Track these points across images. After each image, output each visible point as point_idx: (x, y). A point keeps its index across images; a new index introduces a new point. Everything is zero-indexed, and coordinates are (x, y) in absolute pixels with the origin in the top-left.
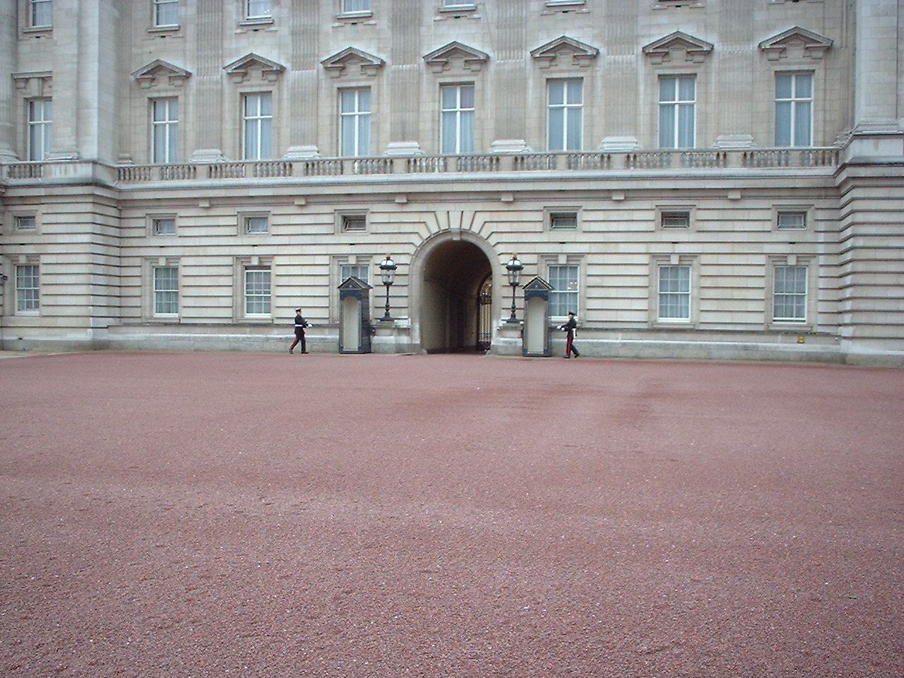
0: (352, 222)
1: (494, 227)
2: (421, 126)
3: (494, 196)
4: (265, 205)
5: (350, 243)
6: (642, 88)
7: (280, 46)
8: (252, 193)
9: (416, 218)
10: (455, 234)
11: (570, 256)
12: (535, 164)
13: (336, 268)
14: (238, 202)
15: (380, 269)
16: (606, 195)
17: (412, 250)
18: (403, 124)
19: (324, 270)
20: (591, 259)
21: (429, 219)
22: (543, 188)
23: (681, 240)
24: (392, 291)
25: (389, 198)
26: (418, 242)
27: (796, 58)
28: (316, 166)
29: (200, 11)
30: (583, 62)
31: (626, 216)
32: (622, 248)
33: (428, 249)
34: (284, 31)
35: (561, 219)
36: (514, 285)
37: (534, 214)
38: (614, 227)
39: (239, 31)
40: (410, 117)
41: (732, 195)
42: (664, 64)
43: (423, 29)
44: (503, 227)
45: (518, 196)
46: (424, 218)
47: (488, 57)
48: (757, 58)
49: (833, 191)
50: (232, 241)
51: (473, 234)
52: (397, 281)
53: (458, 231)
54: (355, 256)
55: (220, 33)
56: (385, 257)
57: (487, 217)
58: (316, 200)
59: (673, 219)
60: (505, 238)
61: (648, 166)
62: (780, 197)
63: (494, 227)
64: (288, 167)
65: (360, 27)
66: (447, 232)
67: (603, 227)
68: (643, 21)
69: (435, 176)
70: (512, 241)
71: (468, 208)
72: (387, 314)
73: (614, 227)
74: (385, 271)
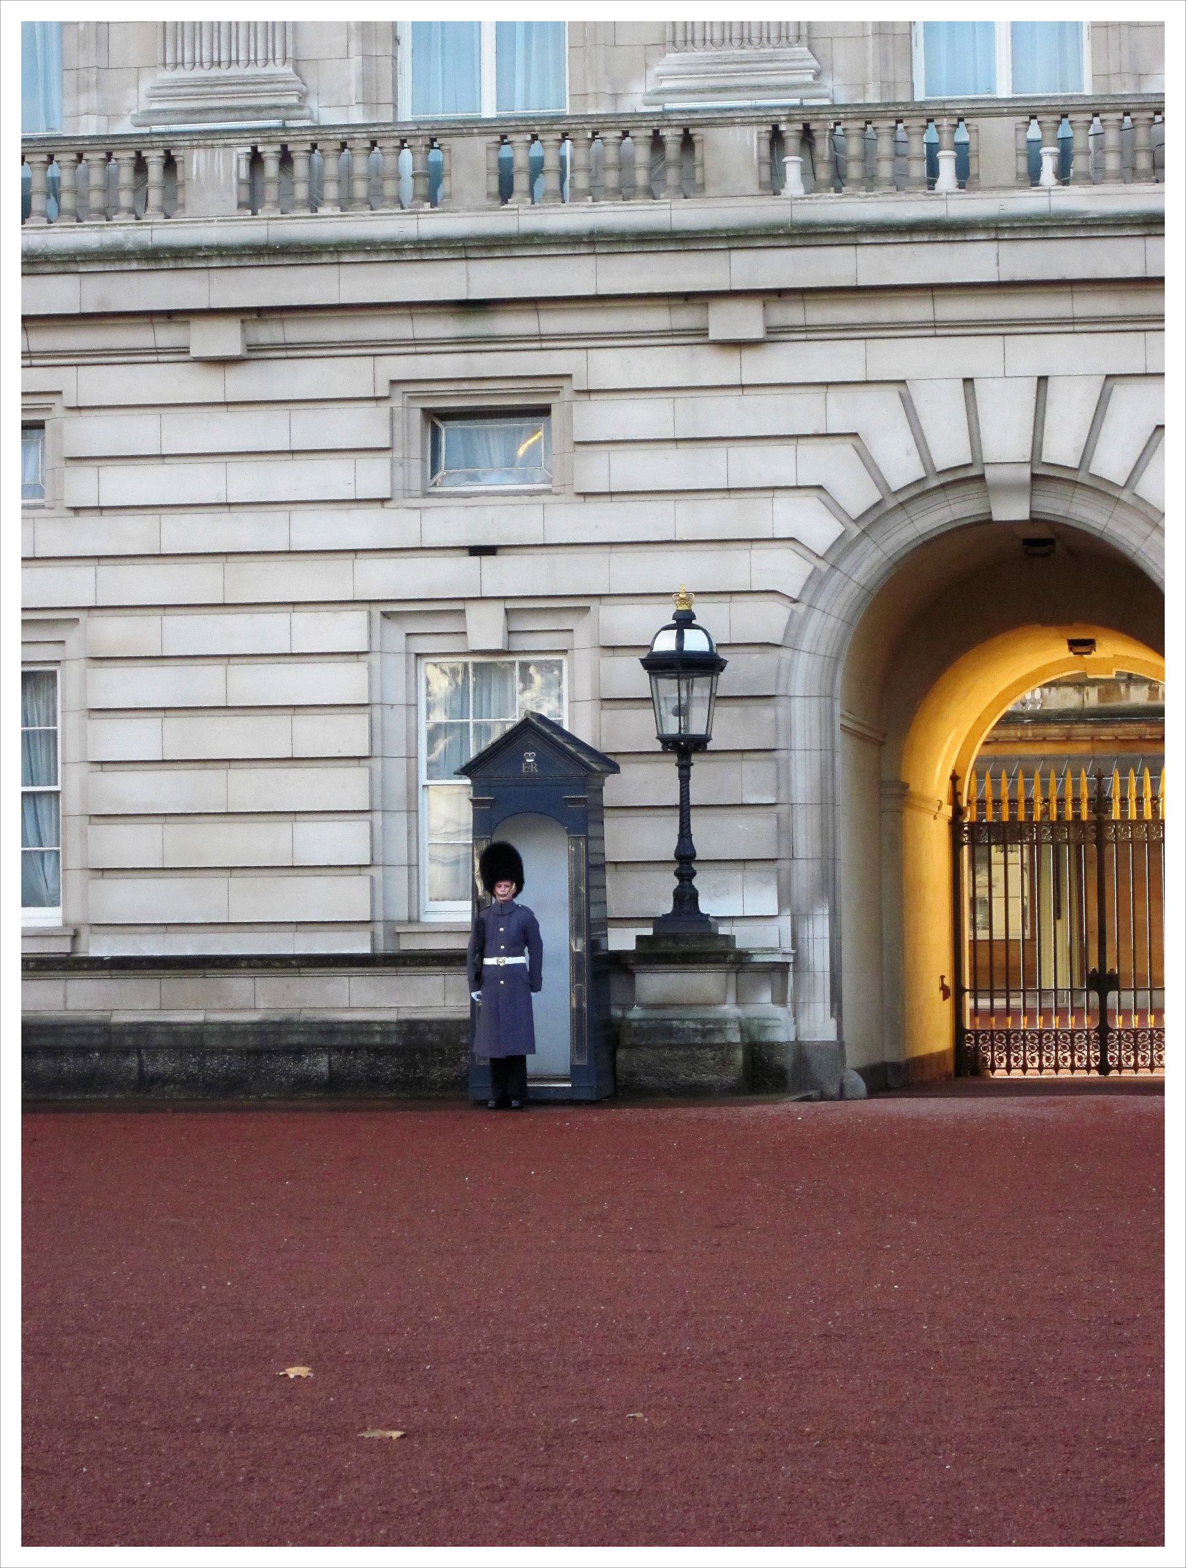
9: (804, 413)
10: (1009, 488)
13: (396, 665)
15: (645, 674)
17: (786, 571)
19: (346, 683)
21: (877, 417)
24: (707, 779)
26: (822, 530)
28: (300, 167)
33: (869, 564)
46: (839, 412)
51: (1101, 490)
52: (727, 729)
53: (1026, 473)
54: (498, 609)
56: (666, 613)
64: (155, 171)
66: (969, 478)
74: (668, 686)
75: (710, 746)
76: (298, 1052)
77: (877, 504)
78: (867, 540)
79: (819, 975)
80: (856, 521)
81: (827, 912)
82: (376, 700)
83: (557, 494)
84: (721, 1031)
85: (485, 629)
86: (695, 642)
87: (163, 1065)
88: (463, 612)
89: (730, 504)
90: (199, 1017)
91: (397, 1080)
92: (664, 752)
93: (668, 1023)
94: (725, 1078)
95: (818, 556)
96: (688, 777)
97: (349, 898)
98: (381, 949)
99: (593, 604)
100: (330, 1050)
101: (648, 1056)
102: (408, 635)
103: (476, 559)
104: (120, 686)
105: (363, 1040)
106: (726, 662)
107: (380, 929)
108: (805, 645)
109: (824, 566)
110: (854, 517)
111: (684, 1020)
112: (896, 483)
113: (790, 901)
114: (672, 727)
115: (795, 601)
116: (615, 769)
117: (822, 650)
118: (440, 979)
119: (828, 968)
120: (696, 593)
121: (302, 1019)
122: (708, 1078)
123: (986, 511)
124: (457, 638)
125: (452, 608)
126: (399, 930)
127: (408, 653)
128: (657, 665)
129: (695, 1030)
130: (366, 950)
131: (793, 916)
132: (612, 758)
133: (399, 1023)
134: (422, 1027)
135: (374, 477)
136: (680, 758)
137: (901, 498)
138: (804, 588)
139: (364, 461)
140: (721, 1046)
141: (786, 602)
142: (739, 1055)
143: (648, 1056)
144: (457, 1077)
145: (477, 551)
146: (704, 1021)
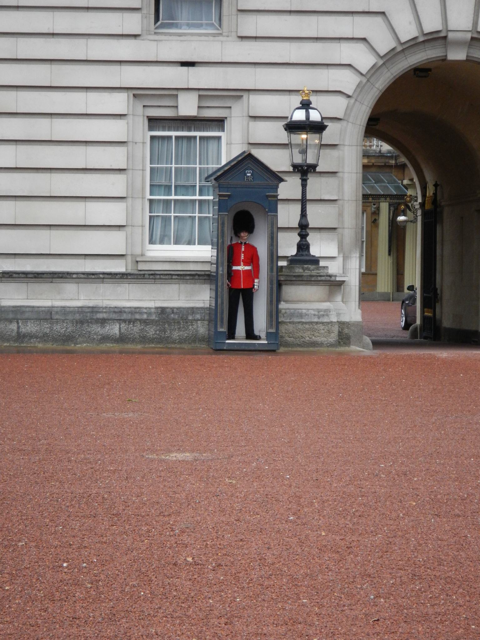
10: (459, 44)
17: (347, 81)
24: (317, 187)
26: (365, 60)
53: (469, 36)
56: (296, 100)
72: (303, 247)
75: (318, 169)
76: (103, 322)
77: (393, 49)
78: (384, 66)
79: (353, 288)
80: (382, 57)
81: (358, 255)
82: (130, 139)
83: (228, 36)
84: (327, 315)
85: (188, 107)
86: (315, 116)
87: (30, 328)
88: (176, 96)
89: (318, 45)
90: (48, 303)
91: (155, 338)
92: (294, 172)
93: (300, 311)
94: (330, 340)
95: (361, 74)
96: (306, 185)
97: (114, 242)
98: (129, 271)
99: (245, 95)
100: (120, 321)
101: (291, 327)
102: (144, 106)
103: (185, 68)
105: (137, 316)
106: (326, 126)
107: (129, 258)
108: (351, 120)
109: (364, 80)
110: (382, 54)
111: (308, 310)
112: (403, 39)
113: (342, 249)
114: (298, 160)
115: (349, 96)
116: (282, 180)
117: (359, 123)
118: (177, 285)
119: (357, 284)
120: (313, 91)
121: (104, 306)
122: (319, 339)
123: (444, 54)
124: (173, 109)
125: (172, 93)
126: (138, 259)
127: (144, 116)
128: (293, 127)
129: (314, 315)
130: (123, 270)
131: (343, 257)
132: (279, 175)
133: (157, 308)
134: (168, 310)
135: (132, 23)
136: (302, 176)
137: (404, 47)
138: (355, 91)
139: (127, 15)
140: (328, 323)
141: (345, 96)
142: (336, 329)
143: (291, 327)
144: (187, 337)
145: (185, 64)
146: (319, 311)
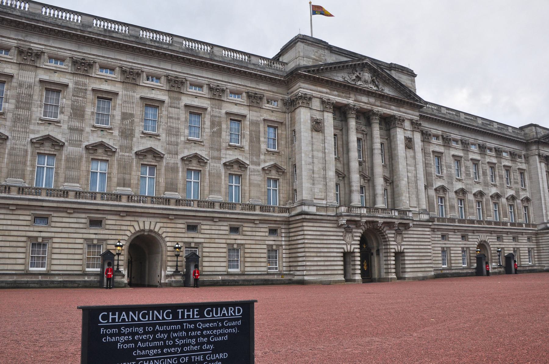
0: (96, 223)
1: (164, 230)
2: (132, 181)
3: (166, 216)
4: (49, 211)
5: (93, 233)
6: (223, 177)
7: (63, 133)
8: (45, 204)
9: (129, 223)
11: (196, 243)
12: (57, 194)
14: (33, 208)
16: (211, 219)
18: (124, 179)
20: (205, 245)
21: (135, 224)
22: (186, 213)
23: (238, 239)
25: (117, 213)
27: (274, 174)
29: (17, 108)
30: (109, 153)
31: (218, 228)
32: (217, 241)
34: (65, 126)
35: (192, 228)
36: (177, 256)
37: (181, 225)
38: (213, 232)
39: (40, 122)
40: (127, 177)
41: (256, 222)
42: (144, 160)
43: (134, 139)
44: (168, 230)
45: (177, 217)
46: (133, 223)
47: (8, 137)
48: (261, 172)
49: (287, 222)
50: (27, 228)
51: (155, 232)
55: (28, 120)
57: (162, 225)
58: (79, 211)
59: (234, 230)
60: (169, 235)
61: (57, 196)
62: (271, 224)
63: (164, 230)
65: (105, 133)
66: (144, 230)
67: (209, 232)
68: (223, 152)
69: (141, 205)
70: (172, 237)
71: (153, 220)
73: (213, 232)
86: (121, 244)
104: (80, 246)
